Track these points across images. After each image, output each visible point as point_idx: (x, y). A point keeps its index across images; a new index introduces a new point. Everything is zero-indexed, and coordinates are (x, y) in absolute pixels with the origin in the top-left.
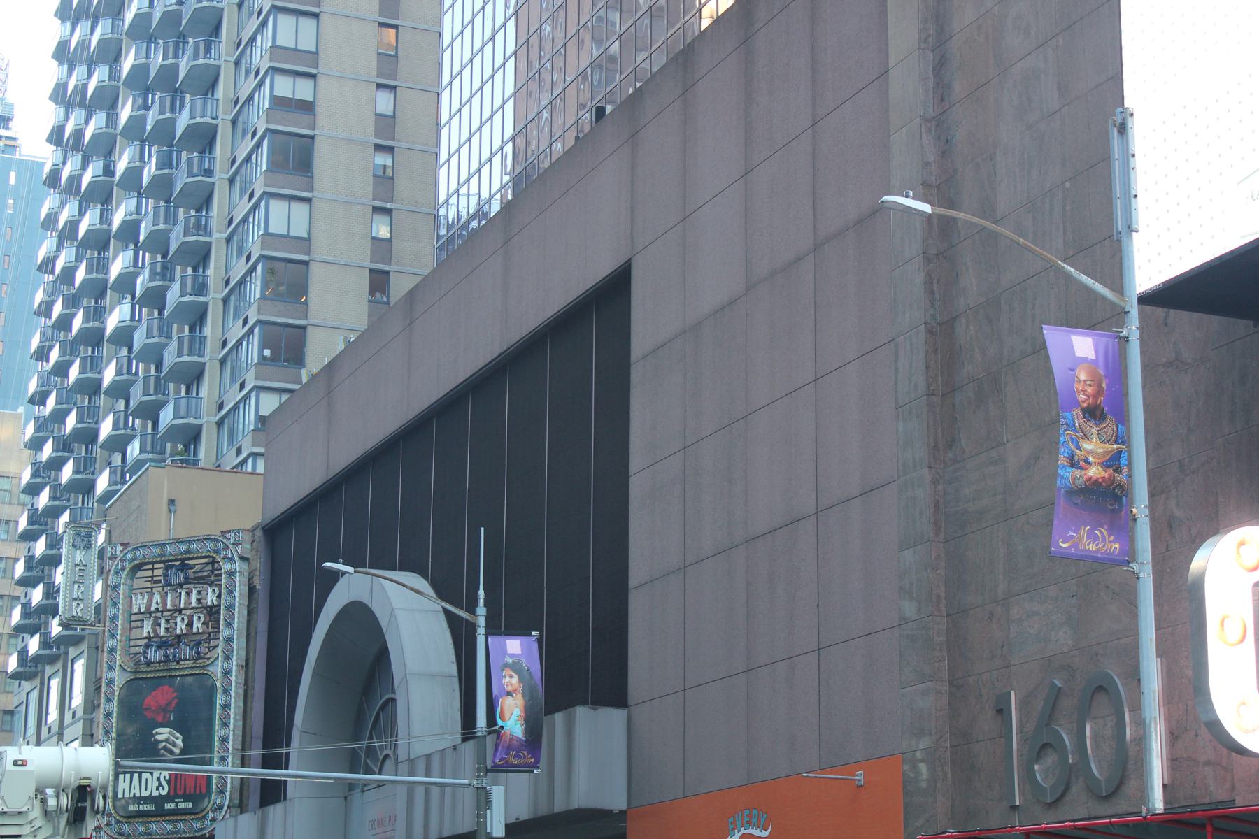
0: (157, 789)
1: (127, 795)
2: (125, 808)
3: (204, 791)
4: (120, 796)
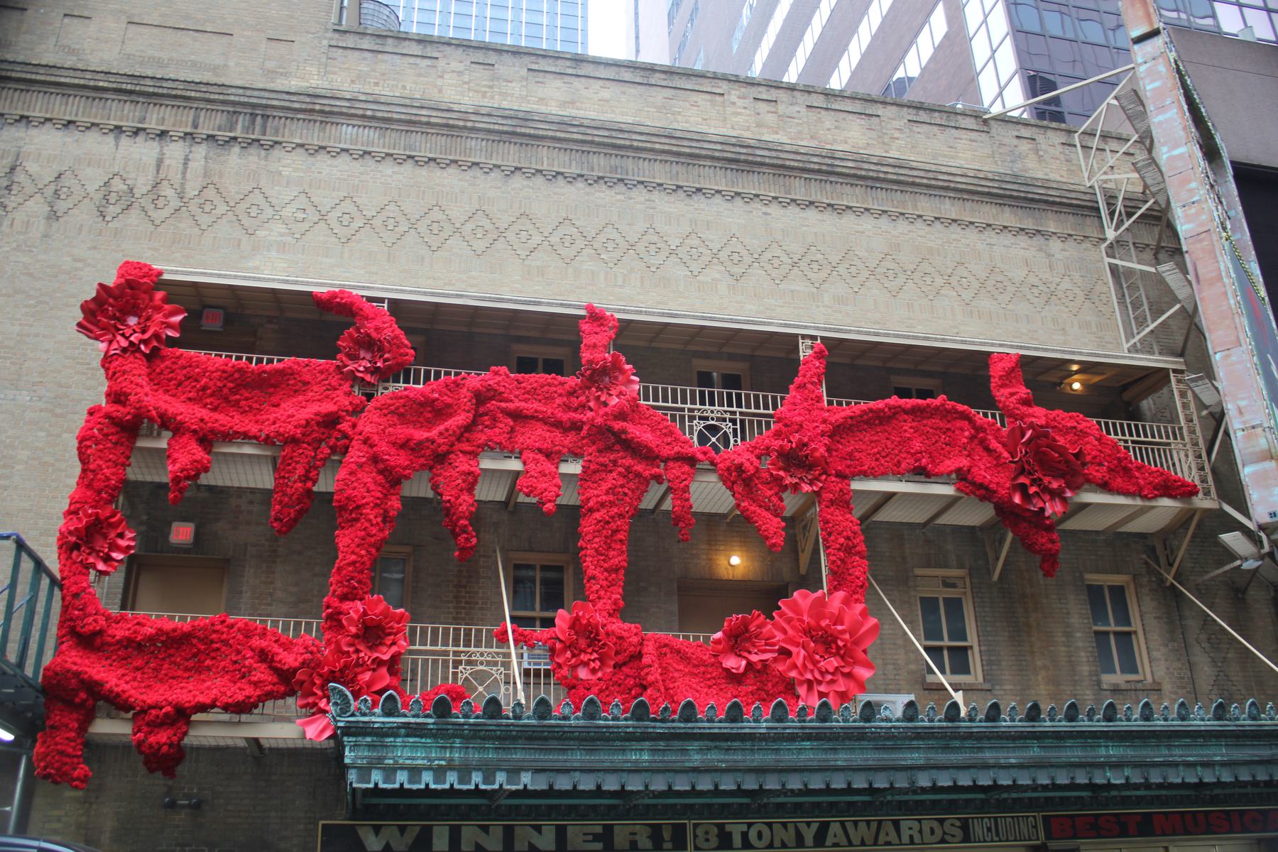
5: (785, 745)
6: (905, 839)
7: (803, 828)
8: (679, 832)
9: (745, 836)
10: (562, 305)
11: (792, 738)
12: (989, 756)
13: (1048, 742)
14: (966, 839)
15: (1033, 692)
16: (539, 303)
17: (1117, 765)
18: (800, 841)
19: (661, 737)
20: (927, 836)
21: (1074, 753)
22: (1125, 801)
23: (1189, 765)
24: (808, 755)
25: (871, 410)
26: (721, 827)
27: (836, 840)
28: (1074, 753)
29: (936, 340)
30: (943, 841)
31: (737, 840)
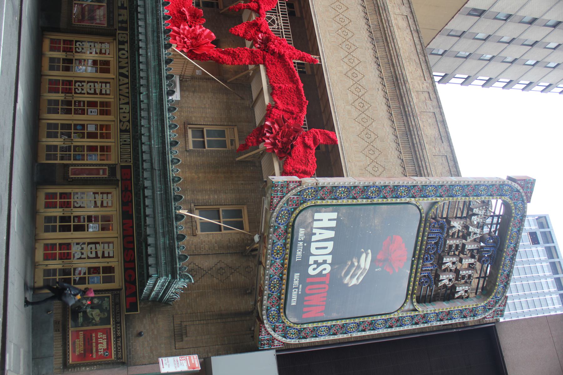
0: (316, 262)
2: (302, 225)
4: (317, 216)
6: (122, 106)
7: (126, 69)
8: (126, 29)
9: (123, 49)
12: (151, 45)
13: (157, 69)
14: (121, 131)
15: (187, 170)
17: (148, 97)
18: (121, 68)
21: (153, 78)
22: (138, 204)
23: (149, 129)
25: (294, 72)
26: (127, 42)
27: (121, 80)
28: (153, 78)
30: (121, 121)
31: (121, 47)
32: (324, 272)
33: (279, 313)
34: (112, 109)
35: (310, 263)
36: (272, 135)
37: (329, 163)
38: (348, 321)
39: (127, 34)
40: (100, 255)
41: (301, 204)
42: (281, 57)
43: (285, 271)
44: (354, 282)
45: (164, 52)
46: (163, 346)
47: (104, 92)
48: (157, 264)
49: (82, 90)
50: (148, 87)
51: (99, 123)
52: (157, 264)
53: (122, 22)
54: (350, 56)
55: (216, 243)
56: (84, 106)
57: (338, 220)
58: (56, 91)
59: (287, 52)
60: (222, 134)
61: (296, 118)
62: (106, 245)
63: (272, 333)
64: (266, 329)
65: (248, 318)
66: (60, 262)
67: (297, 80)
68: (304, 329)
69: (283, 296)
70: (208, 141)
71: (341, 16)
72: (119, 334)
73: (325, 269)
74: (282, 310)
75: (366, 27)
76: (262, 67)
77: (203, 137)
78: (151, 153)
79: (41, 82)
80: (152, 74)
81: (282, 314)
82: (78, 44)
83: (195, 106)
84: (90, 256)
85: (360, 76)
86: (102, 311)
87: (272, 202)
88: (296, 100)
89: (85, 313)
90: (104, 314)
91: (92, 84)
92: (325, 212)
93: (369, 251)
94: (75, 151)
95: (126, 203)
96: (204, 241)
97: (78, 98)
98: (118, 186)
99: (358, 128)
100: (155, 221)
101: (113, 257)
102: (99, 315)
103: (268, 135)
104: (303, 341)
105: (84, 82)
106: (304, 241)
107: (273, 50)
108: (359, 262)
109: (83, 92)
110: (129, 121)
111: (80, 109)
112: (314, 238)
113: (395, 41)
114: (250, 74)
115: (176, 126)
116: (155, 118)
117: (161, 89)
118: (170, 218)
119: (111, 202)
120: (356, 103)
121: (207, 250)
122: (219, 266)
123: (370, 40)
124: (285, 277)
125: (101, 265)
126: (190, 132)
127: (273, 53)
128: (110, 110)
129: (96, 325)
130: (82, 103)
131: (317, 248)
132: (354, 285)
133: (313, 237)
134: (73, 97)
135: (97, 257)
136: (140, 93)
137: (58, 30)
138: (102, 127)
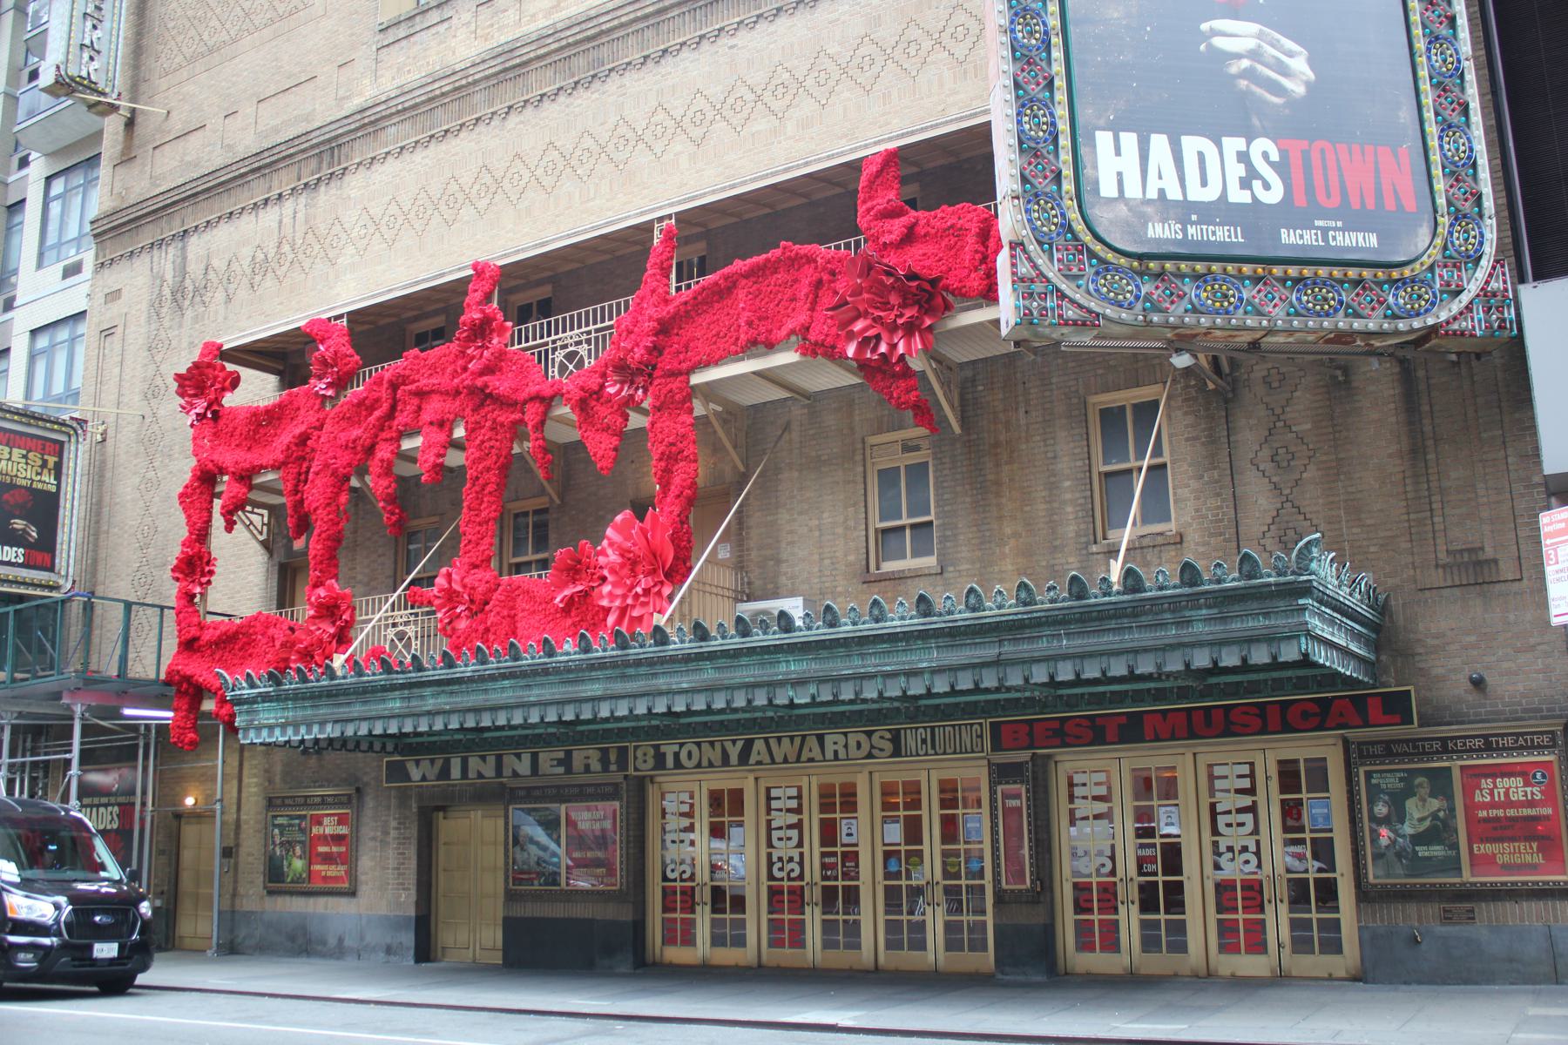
0: (1245, 184)
1: (1133, 191)
3: (1410, 204)
4: (1108, 189)
5: (490, 685)
6: (829, 755)
7: (728, 745)
8: (623, 752)
9: (677, 755)
10: (460, 269)
11: (492, 678)
12: (662, 682)
13: (722, 662)
14: (897, 752)
16: (442, 275)
17: (800, 683)
18: (726, 760)
19: (403, 687)
20: (853, 751)
22: (1098, 700)
23: (888, 675)
24: (505, 693)
25: (704, 288)
27: (759, 758)
28: (749, 672)
29: (798, 167)
30: (870, 756)
31: (670, 762)
32: (1275, 156)
33: (1403, 281)
34: (837, 779)
35: (1249, 201)
36: (884, 336)
37: (949, 170)
38: (1423, 73)
39: (636, 748)
40: (1246, 801)
41: (1076, 238)
42: (664, 328)
43: (1277, 271)
44: (1300, 64)
45: (676, 646)
46: (1512, 617)
47: (793, 804)
48: (1270, 639)
49: (791, 860)
50: (772, 685)
51: (879, 814)
52: (1270, 639)
53: (605, 761)
54: (648, 137)
55: (1202, 477)
56: (834, 854)
57: (1116, 128)
58: (798, 928)
59: (651, 311)
60: (888, 478)
61: (833, 273)
62: (1218, 784)
63: (1465, 298)
64: (1455, 318)
65: (1421, 373)
66: (1270, 909)
67: (726, 278)
68: (1450, 204)
69: (1352, 273)
70: (910, 516)
71: (540, 172)
72: (1479, 743)
73: (1265, 155)
74: (1395, 274)
75: (562, 98)
76: (696, 379)
77: (902, 528)
78: (953, 669)
79: (778, 967)
80: (738, 674)
81: (1407, 272)
82: (670, 875)
83: (816, 557)
84: (1250, 827)
85: (700, 103)
86: (1409, 792)
87: (1075, 323)
88: (780, 277)
89: (1418, 839)
90: (1420, 785)
91: (775, 834)
92: (1095, 167)
93: (1205, 27)
94: (957, 876)
95: (1096, 734)
96: (1197, 511)
97: (813, 871)
98: (1049, 756)
99: (847, 94)
100: (1146, 650)
101: (1252, 764)
102: (1423, 800)
103: (883, 348)
104: (1489, 204)
105: (769, 855)
106: (1185, 222)
107: (649, 351)
108: (1239, 56)
109: (797, 859)
110: (869, 734)
111: (843, 865)
112: (1174, 194)
113: (593, 13)
114: (720, 409)
115: (875, 602)
116: (857, 662)
117: (778, 649)
118: (1136, 607)
119: (1094, 774)
120: (776, 105)
121: (1223, 500)
122: (1267, 466)
123: (597, 84)
124: (1293, 271)
125: (1276, 797)
126: (889, 566)
127: (656, 350)
128: (843, 785)
129: (1452, 810)
130: (827, 860)
131: (1204, 183)
132: (1311, 62)
133: (1170, 197)
134: (812, 884)
135: (1252, 809)
136: (792, 705)
137: (639, 927)
138: (886, 806)
